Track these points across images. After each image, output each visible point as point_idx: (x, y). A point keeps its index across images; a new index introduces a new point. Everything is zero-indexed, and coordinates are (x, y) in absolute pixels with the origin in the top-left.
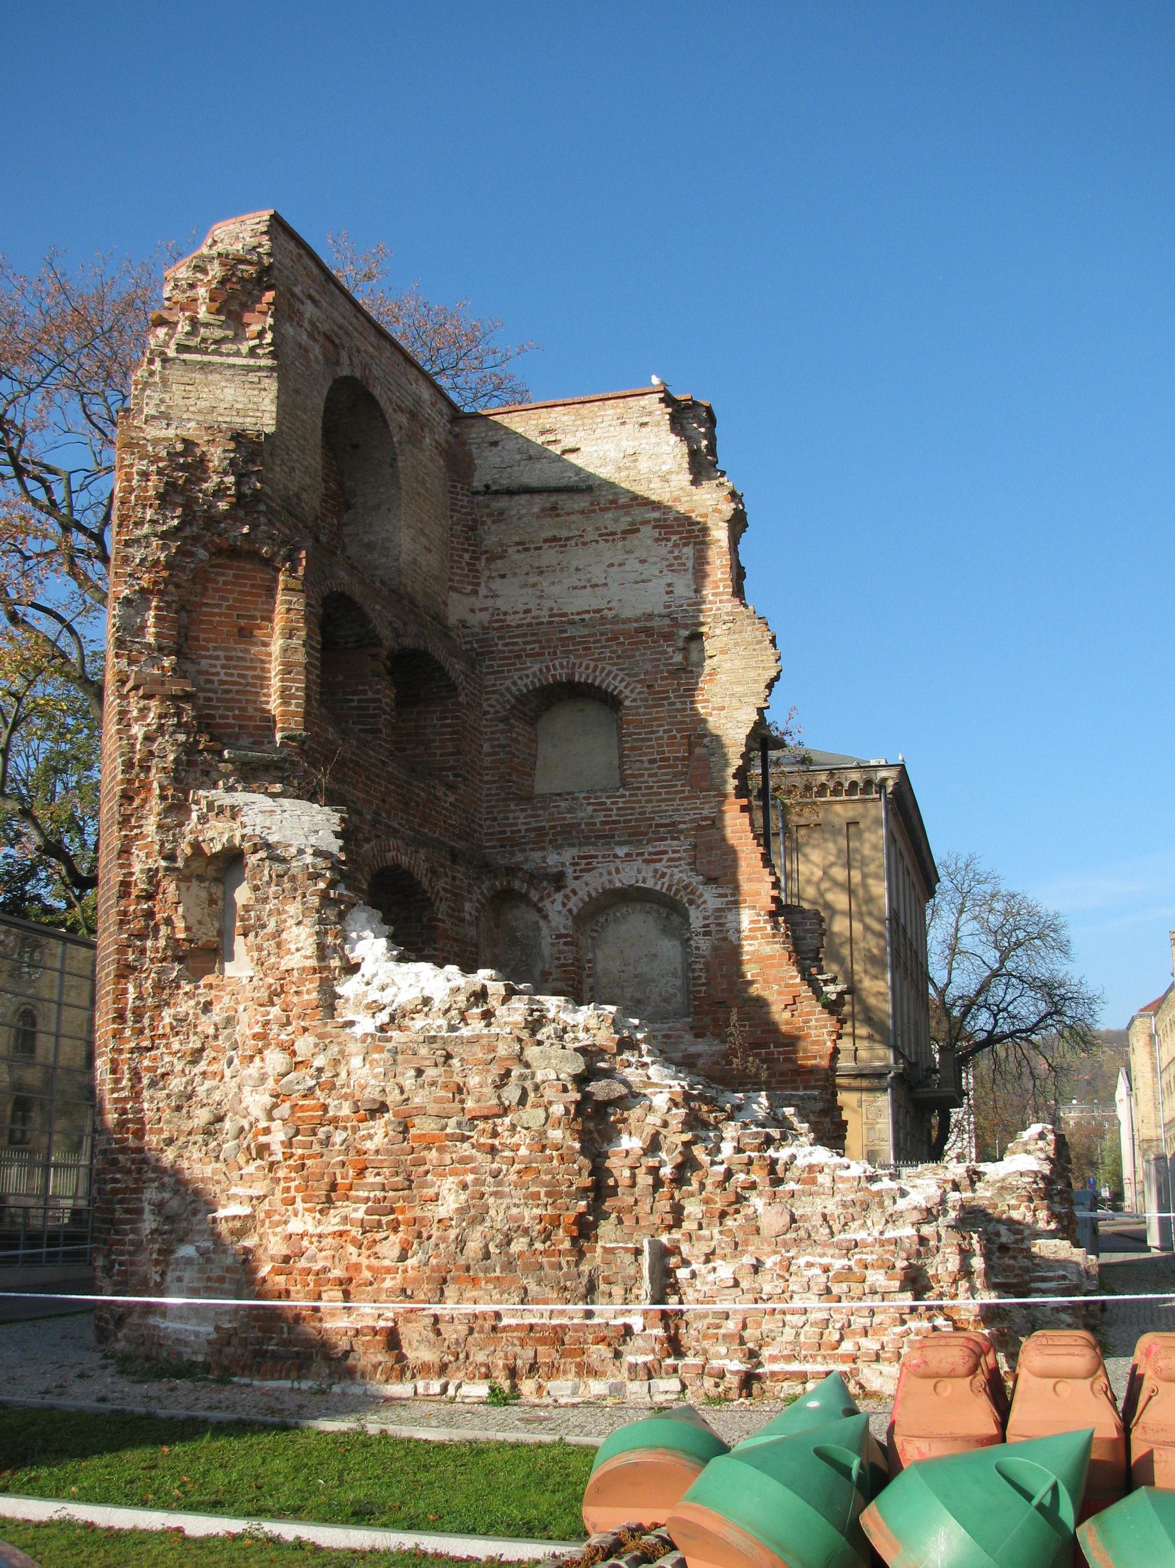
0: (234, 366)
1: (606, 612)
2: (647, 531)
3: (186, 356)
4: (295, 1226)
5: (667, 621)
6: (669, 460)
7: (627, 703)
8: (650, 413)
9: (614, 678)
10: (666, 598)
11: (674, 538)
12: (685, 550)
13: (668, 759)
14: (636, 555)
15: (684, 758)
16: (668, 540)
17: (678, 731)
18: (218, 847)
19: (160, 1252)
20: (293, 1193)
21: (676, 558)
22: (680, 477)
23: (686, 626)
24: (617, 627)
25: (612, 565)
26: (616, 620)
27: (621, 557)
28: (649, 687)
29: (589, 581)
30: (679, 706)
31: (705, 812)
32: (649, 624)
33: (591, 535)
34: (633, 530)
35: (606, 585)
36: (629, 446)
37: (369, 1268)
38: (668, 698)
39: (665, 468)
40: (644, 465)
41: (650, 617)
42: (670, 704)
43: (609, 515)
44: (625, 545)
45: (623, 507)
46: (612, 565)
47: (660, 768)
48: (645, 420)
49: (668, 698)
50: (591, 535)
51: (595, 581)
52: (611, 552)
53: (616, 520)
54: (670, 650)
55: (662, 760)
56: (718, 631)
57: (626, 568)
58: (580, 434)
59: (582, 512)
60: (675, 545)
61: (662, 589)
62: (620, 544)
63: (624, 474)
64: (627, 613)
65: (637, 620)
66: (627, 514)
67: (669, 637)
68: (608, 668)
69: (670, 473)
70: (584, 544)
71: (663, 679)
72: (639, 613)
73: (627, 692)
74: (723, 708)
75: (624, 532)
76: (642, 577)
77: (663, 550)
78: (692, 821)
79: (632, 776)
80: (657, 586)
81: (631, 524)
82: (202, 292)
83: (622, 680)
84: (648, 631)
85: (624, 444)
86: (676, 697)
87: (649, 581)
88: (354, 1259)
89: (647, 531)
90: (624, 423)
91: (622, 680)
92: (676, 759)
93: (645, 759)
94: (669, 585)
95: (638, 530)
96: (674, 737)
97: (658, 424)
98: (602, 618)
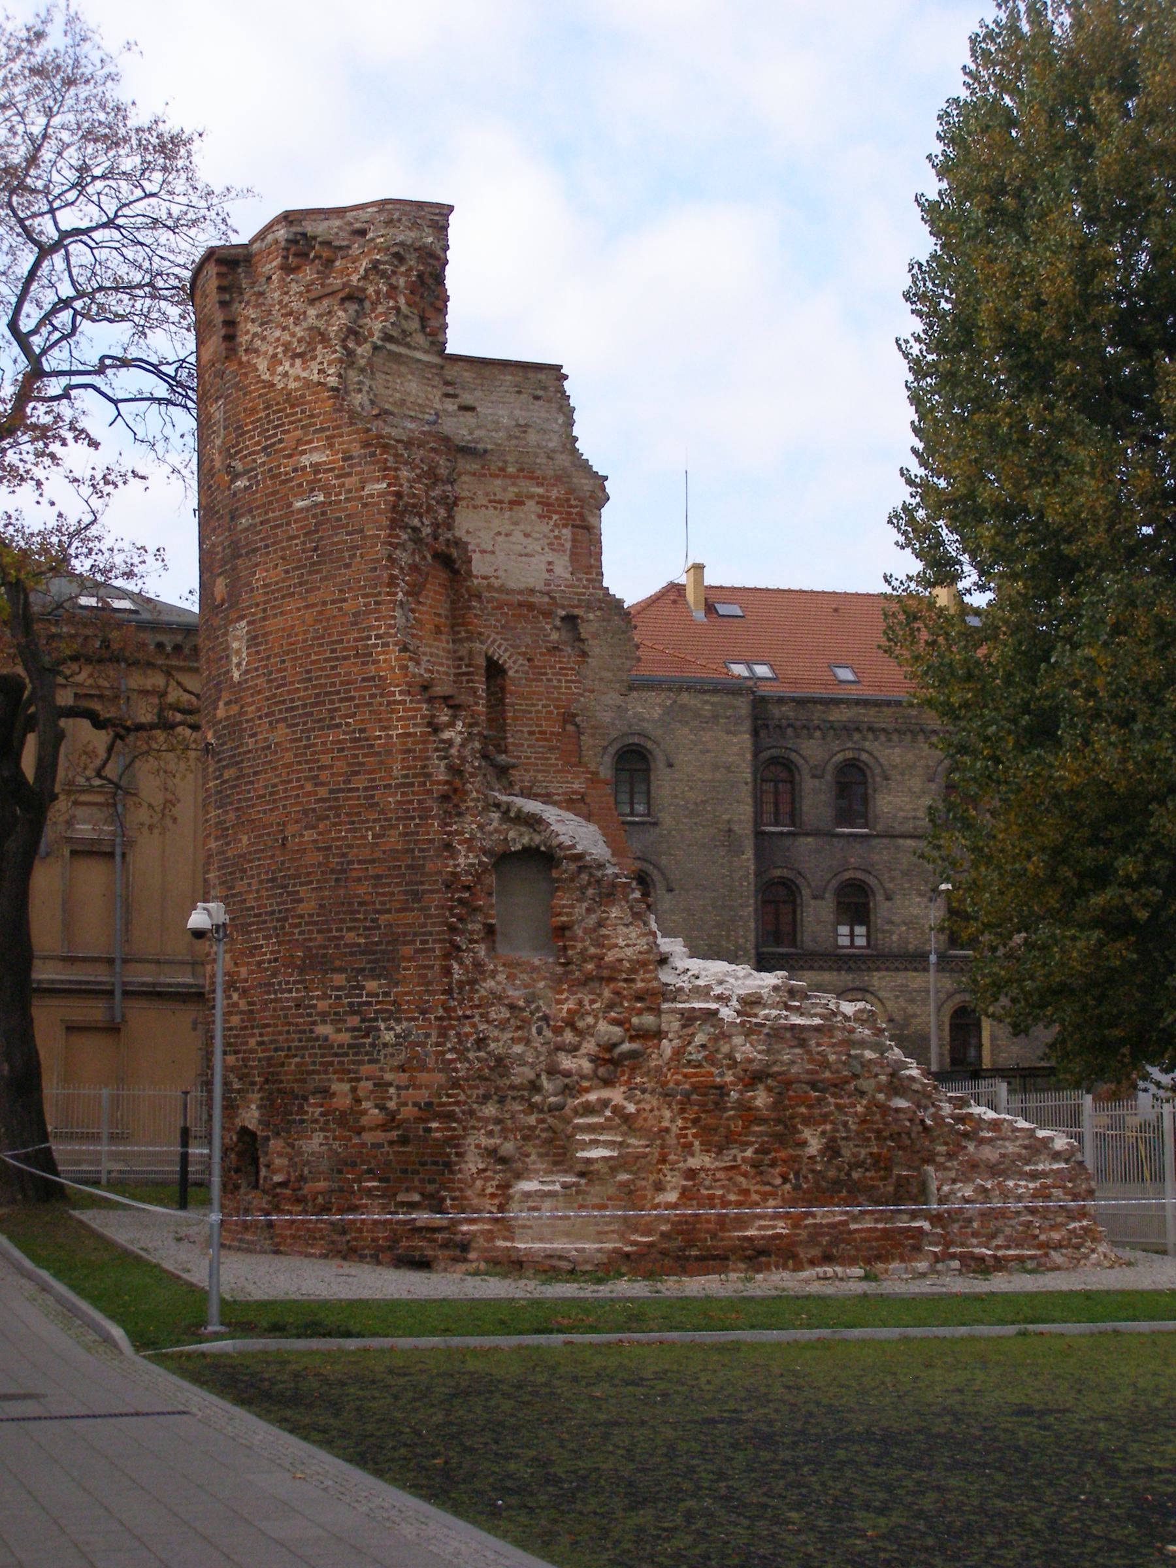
0: (419, 361)
1: (492, 580)
2: (531, 505)
3: (390, 346)
4: (693, 1162)
5: (546, 599)
6: (555, 438)
7: (511, 673)
8: (545, 388)
9: (499, 647)
10: (547, 576)
11: (555, 517)
12: (564, 531)
13: (544, 733)
14: (522, 527)
15: (559, 734)
16: (550, 518)
17: (557, 707)
18: (519, 847)
19: (498, 1187)
20: (690, 1138)
21: (556, 537)
22: (563, 457)
23: (563, 607)
24: (504, 597)
25: (499, 534)
26: (502, 589)
27: (508, 527)
28: (529, 660)
29: (478, 545)
30: (555, 683)
31: (575, 786)
32: (532, 599)
33: (481, 500)
34: (517, 502)
35: (493, 552)
36: (521, 416)
37: (757, 1192)
38: (545, 674)
39: (551, 445)
40: (532, 437)
41: (532, 591)
42: (549, 680)
43: (499, 482)
44: (511, 518)
45: (511, 476)
46: (499, 534)
47: (537, 740)
48: (539, 393)
49: (545, 674)
50: (481, 500)
51: (484, 546)
52: (499, 521)
53: (504, 490)
54: (548, 627)
55: (540, 732)
56: (591, 616)
57: (513, 539)
58: (478, 394)
59: (474, 474)
60: (556, 525)
61: (544, 567)
62: (508, 514)
63: (514, 442)
64: (512, 585)
65: (520, 592)
66: (514, 484)
67: (548, 614)
68: (493, 636)
69: (554, 451)
70: (475, 507)
71: (542, 654)
72: (522, 586)
73: (510, 663)
74: (592, 691)
75: (512, 503)
76: (527, 551)
77: (545, 527)
78: (565, 794)
79: (513, 744)
80: (538, 563)
81: (517, 495)
82: (402, 282)
83: (506, 650)
84: (531, 607)
85: (517, 412)
86: (554, 674)
87: (532, 556)
88: (744, 1186)
89: (531, 505)
90: (519, 392)
91: (506, 650)
92: (552, 733)
93: (526, 729)
94: (550, 563)
95: (522, 503)
96: (551, 712)
97: (550, 401)
98: (489, 585)
